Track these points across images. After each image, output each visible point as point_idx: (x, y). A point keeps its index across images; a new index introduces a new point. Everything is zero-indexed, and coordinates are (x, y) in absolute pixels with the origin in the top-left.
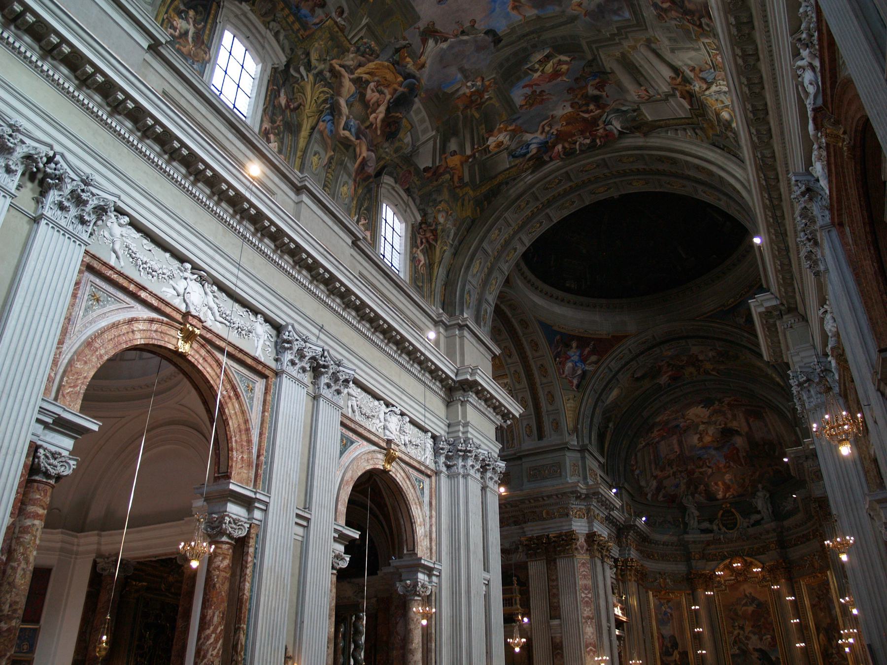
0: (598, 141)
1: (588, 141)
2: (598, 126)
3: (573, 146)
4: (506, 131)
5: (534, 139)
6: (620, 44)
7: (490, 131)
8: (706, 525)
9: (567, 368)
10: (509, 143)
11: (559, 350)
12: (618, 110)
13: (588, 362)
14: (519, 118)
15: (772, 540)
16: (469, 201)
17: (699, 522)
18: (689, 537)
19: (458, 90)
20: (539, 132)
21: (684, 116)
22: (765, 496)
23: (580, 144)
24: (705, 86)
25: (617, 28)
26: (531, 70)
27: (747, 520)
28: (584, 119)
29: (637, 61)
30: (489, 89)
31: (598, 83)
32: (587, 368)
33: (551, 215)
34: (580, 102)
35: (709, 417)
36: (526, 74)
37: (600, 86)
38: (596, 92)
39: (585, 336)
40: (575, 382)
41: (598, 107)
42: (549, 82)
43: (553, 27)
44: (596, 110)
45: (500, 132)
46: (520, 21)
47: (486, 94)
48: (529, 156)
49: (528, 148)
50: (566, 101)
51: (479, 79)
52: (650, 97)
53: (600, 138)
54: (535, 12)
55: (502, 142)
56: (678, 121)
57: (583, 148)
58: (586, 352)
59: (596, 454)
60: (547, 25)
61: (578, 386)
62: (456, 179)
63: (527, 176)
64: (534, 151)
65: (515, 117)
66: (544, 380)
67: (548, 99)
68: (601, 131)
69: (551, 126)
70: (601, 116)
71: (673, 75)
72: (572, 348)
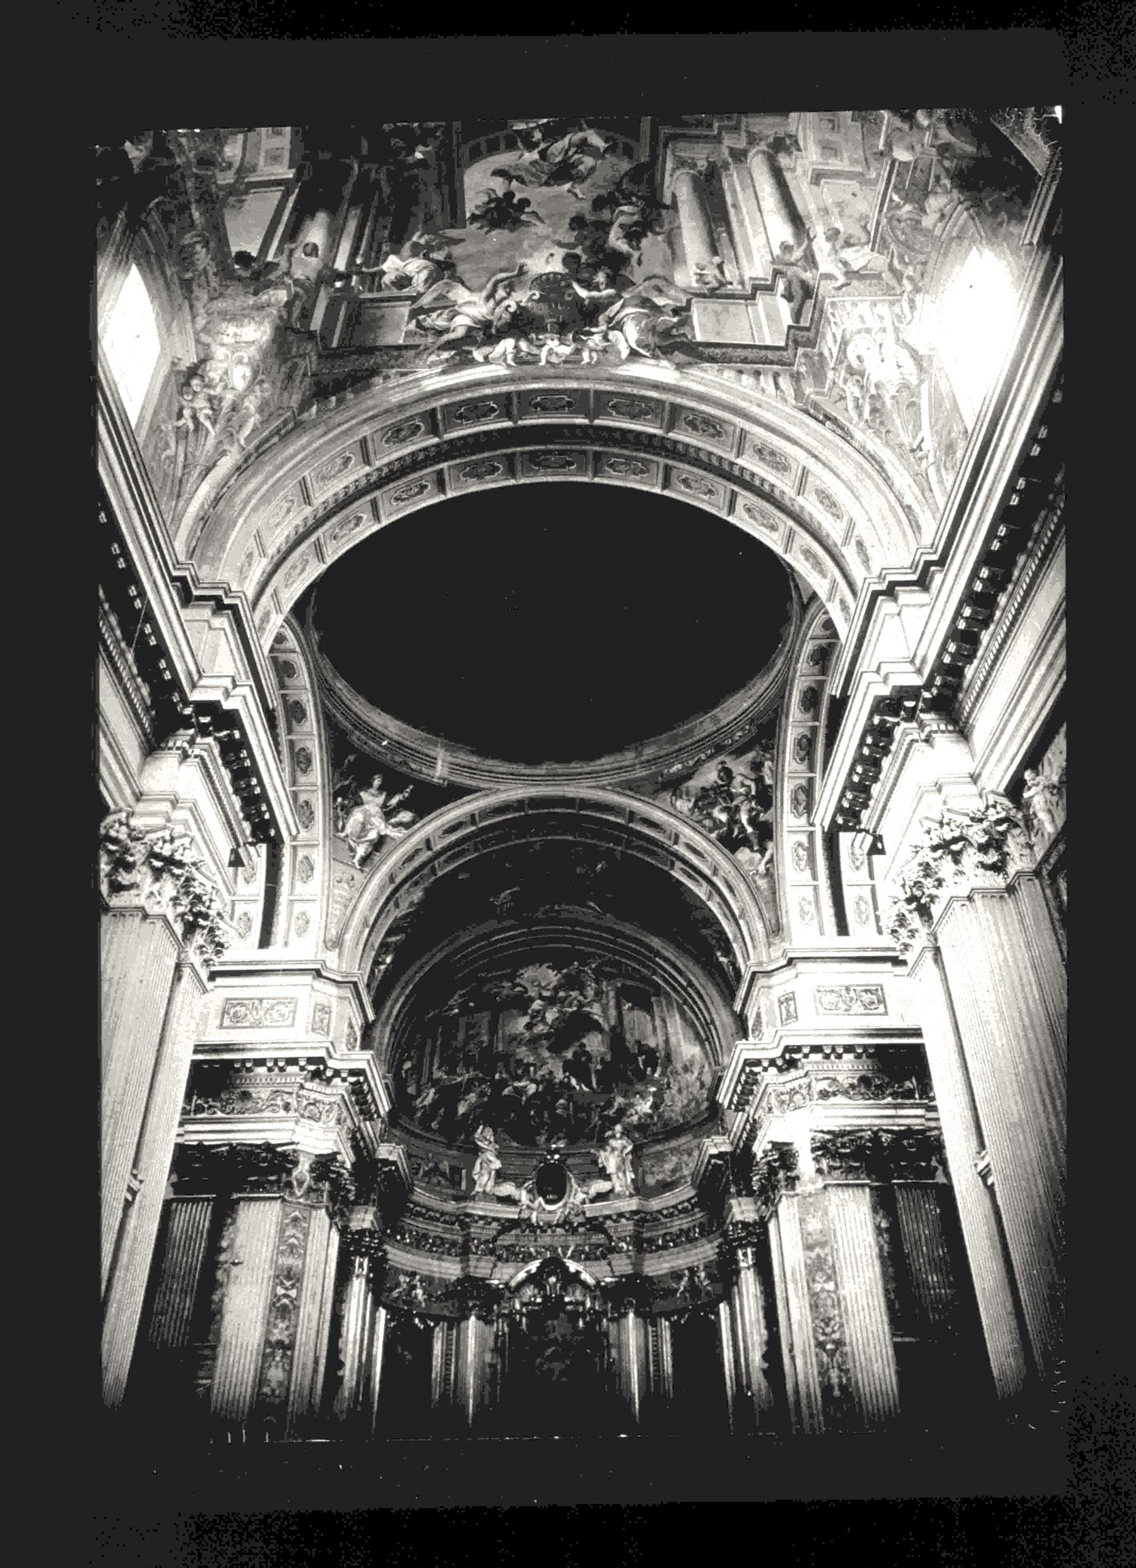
0: (586, 355)
1: (566, 350)
2: (597, 325)
3: (535, 351)
4: (426, 257)
7: (396, 243)
8: (507, 1189)
10: (421, 289)
11: (347, 783)
13: (393, 821)
15: (624, 1234)
17: (497, 1183)
18: (478, 1209)
20: (484, 293)
22: (625, 1147)
23: (551, 352)
27: (585, 1189)
30: (430, 140)
31: (636, 224)
33: (447, 477)
34: (584, 258)
35: (556, 989)
36: (511, 146)
38: (623, 246)
40: (361, 851)
41: (611, 282)
42: (547, 184)
44: (607, 286)
45: (415, 254)
47: (421, 148)
48: (446, 337)
49: (451, 319)
50: (560, 244)
53: (591, 350)
57: (554, 359)
58: (394, 801)
59: (366, 1000)
61: (364, 861)
62: (296, 313)
63: (430, 377)
64: (460, 333)
68: (597, 338)
69: (511, 288)
70: (612, 304)
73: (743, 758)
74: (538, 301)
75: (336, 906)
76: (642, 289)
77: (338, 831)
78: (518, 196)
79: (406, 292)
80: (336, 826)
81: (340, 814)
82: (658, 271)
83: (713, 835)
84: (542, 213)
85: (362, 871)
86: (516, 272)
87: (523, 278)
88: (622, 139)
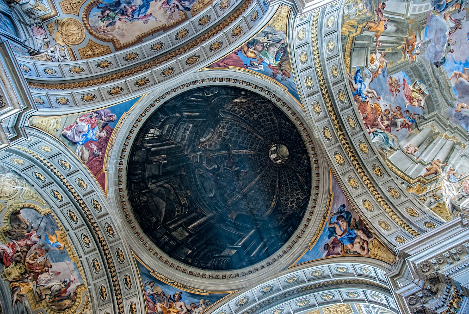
5: (365, 87)
6: (446, 131)
9: (84, 124)
11: (103, 117)
12: (388, 139)
13: (84, 148)
14: (384, 76)
16: (350, 32)
19: (420, 37)
21: (409, 175)
24: (446, 178)
25: (456, 128)
26: (415, 84)
28: (376, 119)
29: (438, 141)
31: (407, 124)
32: (78, 147)
36: (412, 81)
37: (404, 125)
38: (399, 124)
39: (108, 147)
40: (69, 133)
42: (406, 95)
43: (443, 95)
45: (381, 62)
46: (448, 77)
48: (353, 82)
50: (390, 106)
51: (419, 52)
52: (412, 154)
54: (453, 85)
55: (373, 63)
56: (399, 173)
58: (94, 147)
60: (444, 92)
61: (65, 136)
65: (386, 73)
66: (78, 98)
67: (393, 95)
68: (368, 130)
70: (380, 129)
71: (441, 161)
72: (101, 131)
73: (191, 298)
74: (371, 108)
75: (46, 122)
76: (390, 135)
77: (80, 117)
78: (400, 89)
79: (369, 63)
80: (83, 116)
81: (88, 117)
82: (399, 136)
83: (149, 311)
84: (398, 97)
85: (60, 136)
86: (377, 97)
87: (376, 100)
88: (426, 109)
